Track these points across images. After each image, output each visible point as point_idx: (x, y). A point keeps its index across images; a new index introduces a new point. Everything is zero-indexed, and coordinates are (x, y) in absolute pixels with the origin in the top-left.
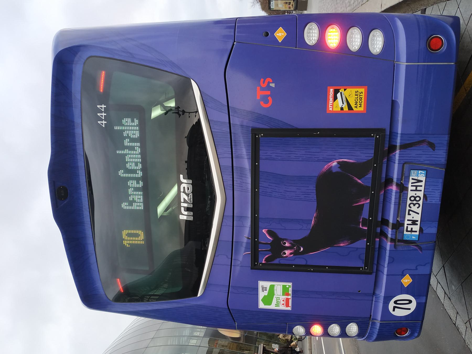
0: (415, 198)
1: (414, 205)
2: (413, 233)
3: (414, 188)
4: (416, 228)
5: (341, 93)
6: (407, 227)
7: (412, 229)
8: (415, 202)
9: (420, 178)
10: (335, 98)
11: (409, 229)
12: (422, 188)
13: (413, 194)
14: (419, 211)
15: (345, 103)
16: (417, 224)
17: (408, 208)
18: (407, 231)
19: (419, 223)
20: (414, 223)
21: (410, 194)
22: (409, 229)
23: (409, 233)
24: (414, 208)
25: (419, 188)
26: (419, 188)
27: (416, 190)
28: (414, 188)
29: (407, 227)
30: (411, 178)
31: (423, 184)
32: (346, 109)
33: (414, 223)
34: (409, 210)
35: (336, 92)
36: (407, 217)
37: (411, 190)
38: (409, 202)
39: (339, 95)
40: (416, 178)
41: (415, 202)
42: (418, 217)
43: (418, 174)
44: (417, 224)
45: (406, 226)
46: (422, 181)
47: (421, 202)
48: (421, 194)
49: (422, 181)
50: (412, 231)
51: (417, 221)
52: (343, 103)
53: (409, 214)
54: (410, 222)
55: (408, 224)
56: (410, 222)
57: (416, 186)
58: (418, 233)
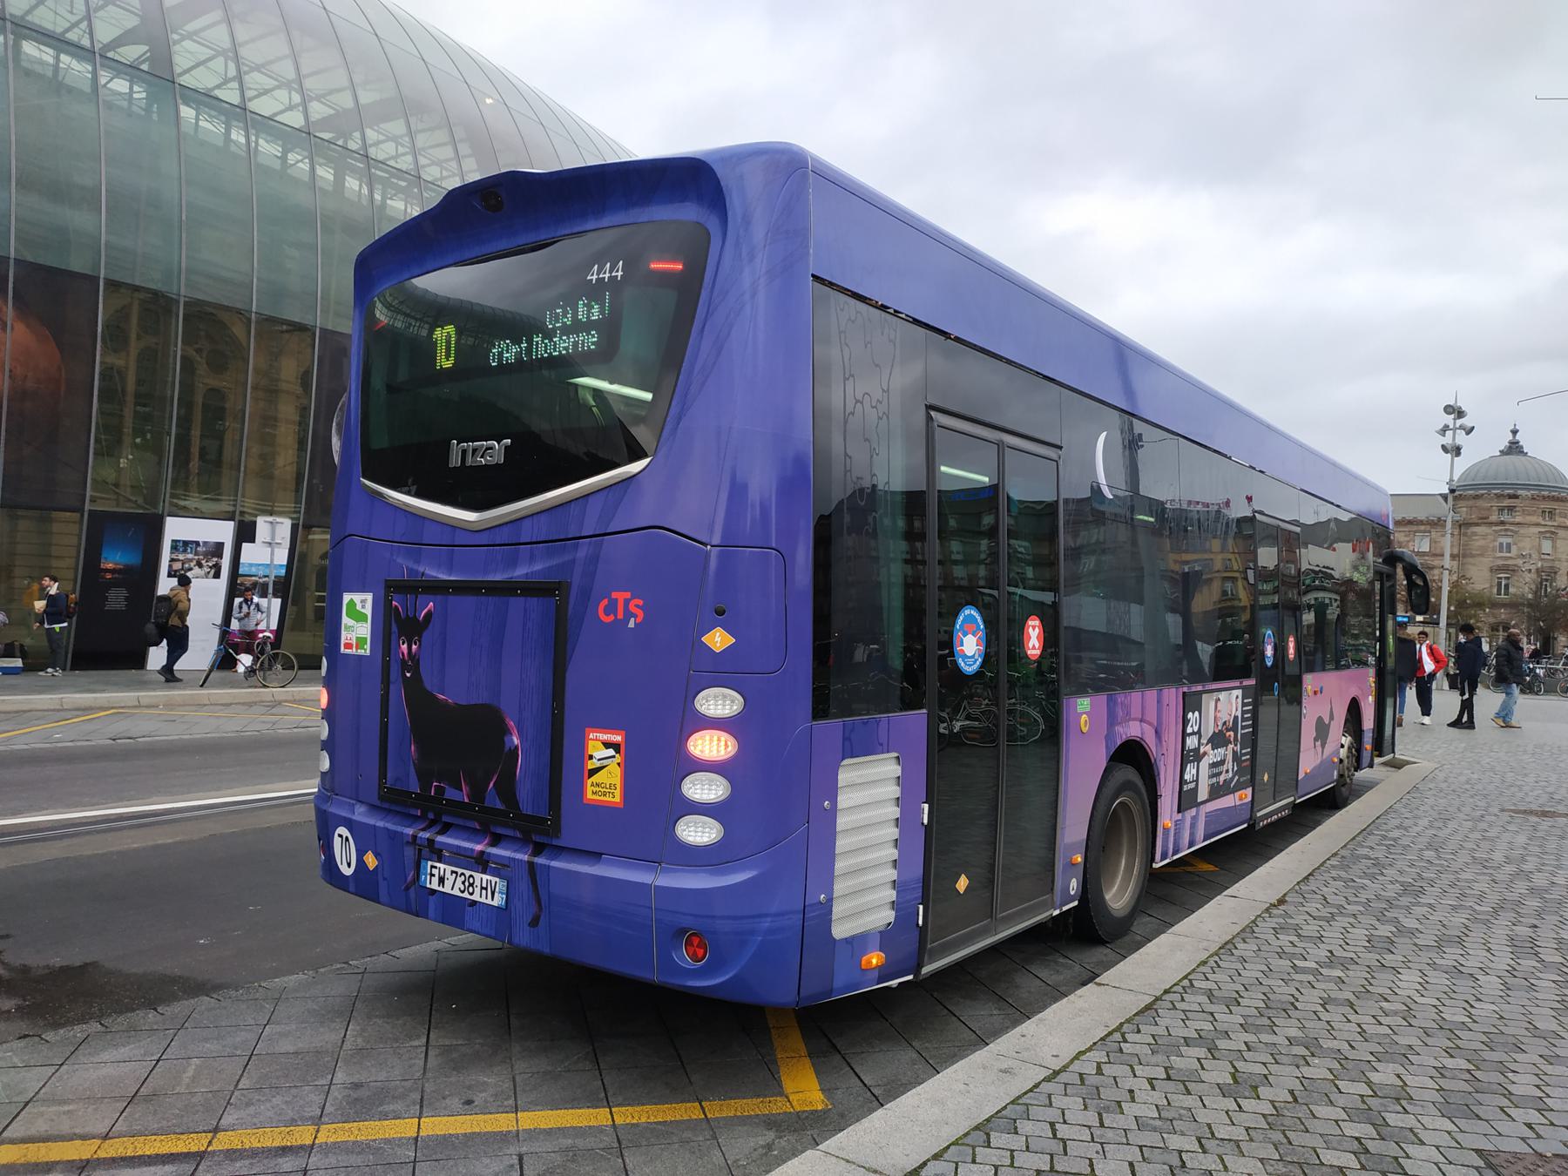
0: (471, 885)
1: (463, 883)
2: (428, 877)
3: (484, 885)
4: (435, 885)
5: (614, 757)
6: (436, 867)
7: (434, 875)
8: (467, 884)
9: (496, 894)
10: (607, 745)
12: (483, 900)
13: (477, 883)
14: (456, 892)
15: (598, 764)
17: (460, 871)
18: (432, 867)
19: (440, 889)
20: (442, 880)
21: (477, 876)
22: (435, 871)
23: (429, 871)
24: (459, 884)
25: (484, 892)
27: (482, 888)
29: (436, 867)
30: (498, 880)
31: (489, 901)
32: (591, 765)
33: (442, 880)
34: (456, 873)
35: (615, 746)
36: (449, 868)
38: (468, 873)
39: (611, 752)
40: (497, 889)
41: (467, 884)
42: (447, 889)
43: (502, 893)
45: (438, 865)
47: (466, 895)
48: (476, 897)
49: (493, 900)
51: (443, 887)
52: (599, 760)
53: (453, 872)
54: (442, 873)
56: (442, 873)
57: (486, 889)
58: (428, 886)
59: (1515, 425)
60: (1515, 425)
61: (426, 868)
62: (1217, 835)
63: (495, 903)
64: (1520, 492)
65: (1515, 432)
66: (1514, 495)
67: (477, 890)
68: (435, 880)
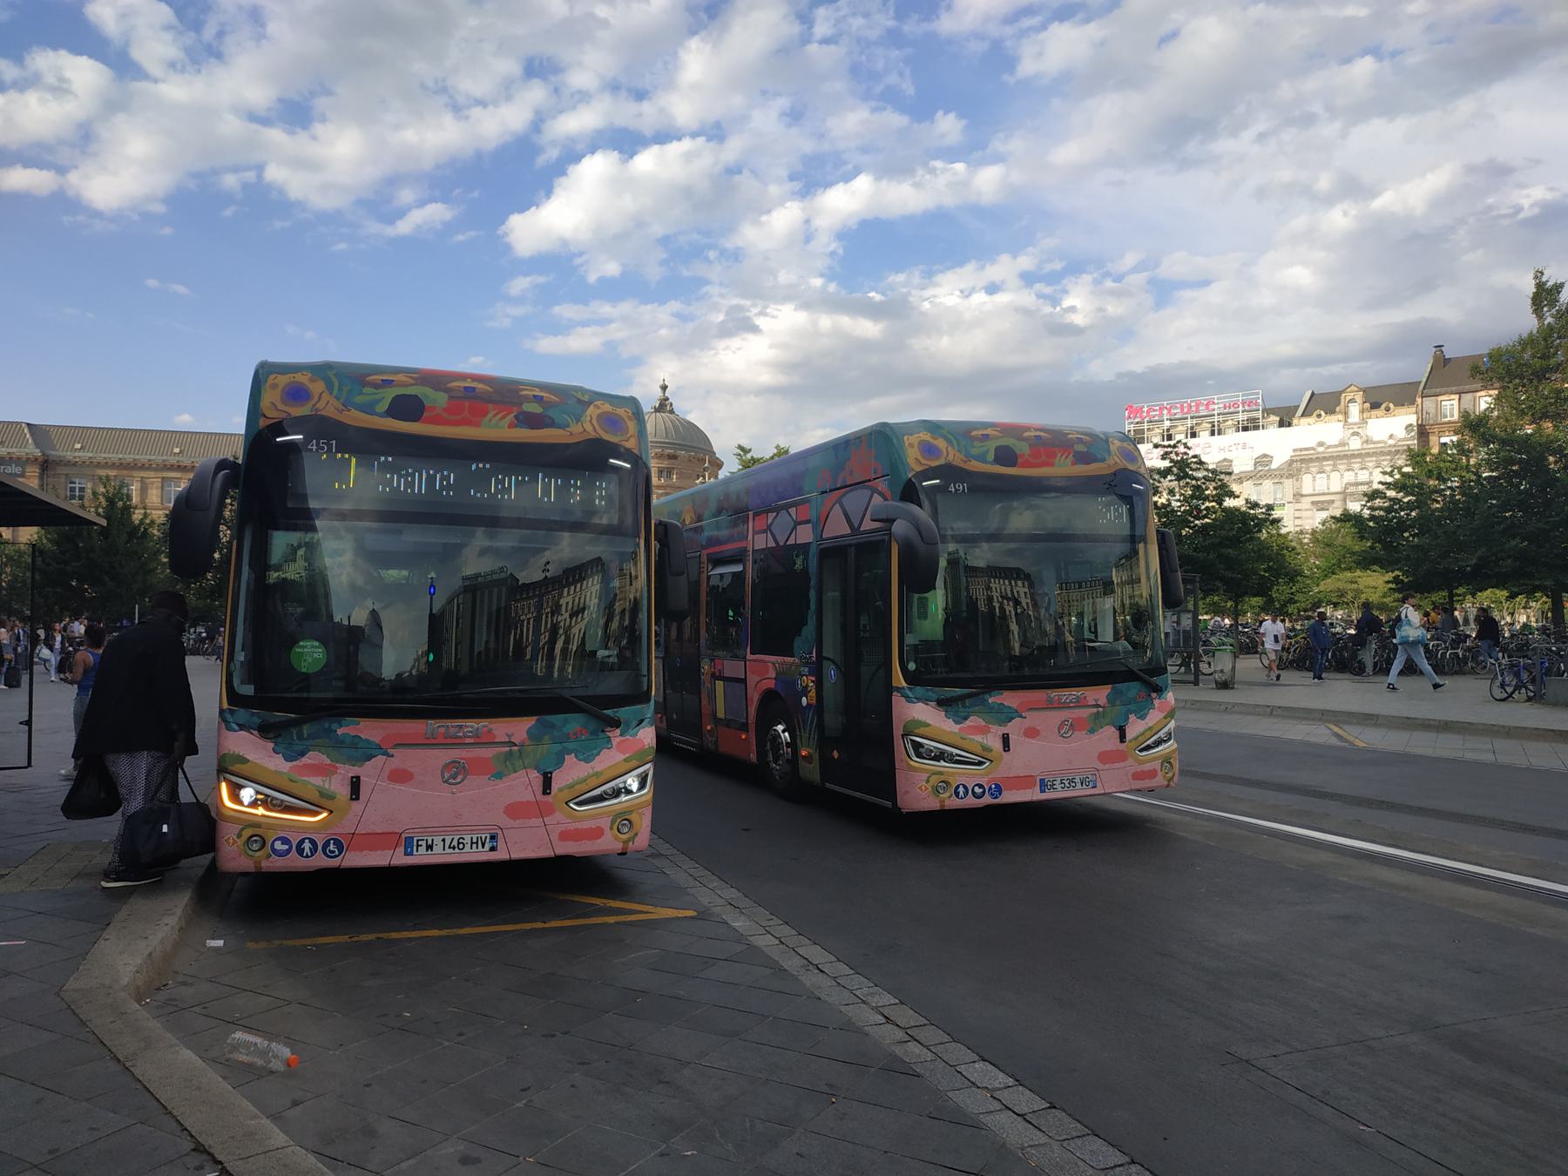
2: (415, 848)
3: (475, 840)
11: (420, 843)
16: (427, 850)
18: (418, 841)
20: (429, 847)
22: (420, 843)
23: (415, 843)
25: (474, 846)
26: (474, 846)
27: (472, 843)
28: (475, 840)
33: (429, 847)
37: (472, 838)
44: (427, 850)
46: (483, 847)
49: (483, 847)
51: (432, 850)
54: (430, 842)
55: (427, 840)
56: (430, 842)
57: (477, 843)
59: (664, 380)
60: (664, 380)
64: (679, 452)
65: (664, 388)
66: (674, 456)
68: (422, 850)
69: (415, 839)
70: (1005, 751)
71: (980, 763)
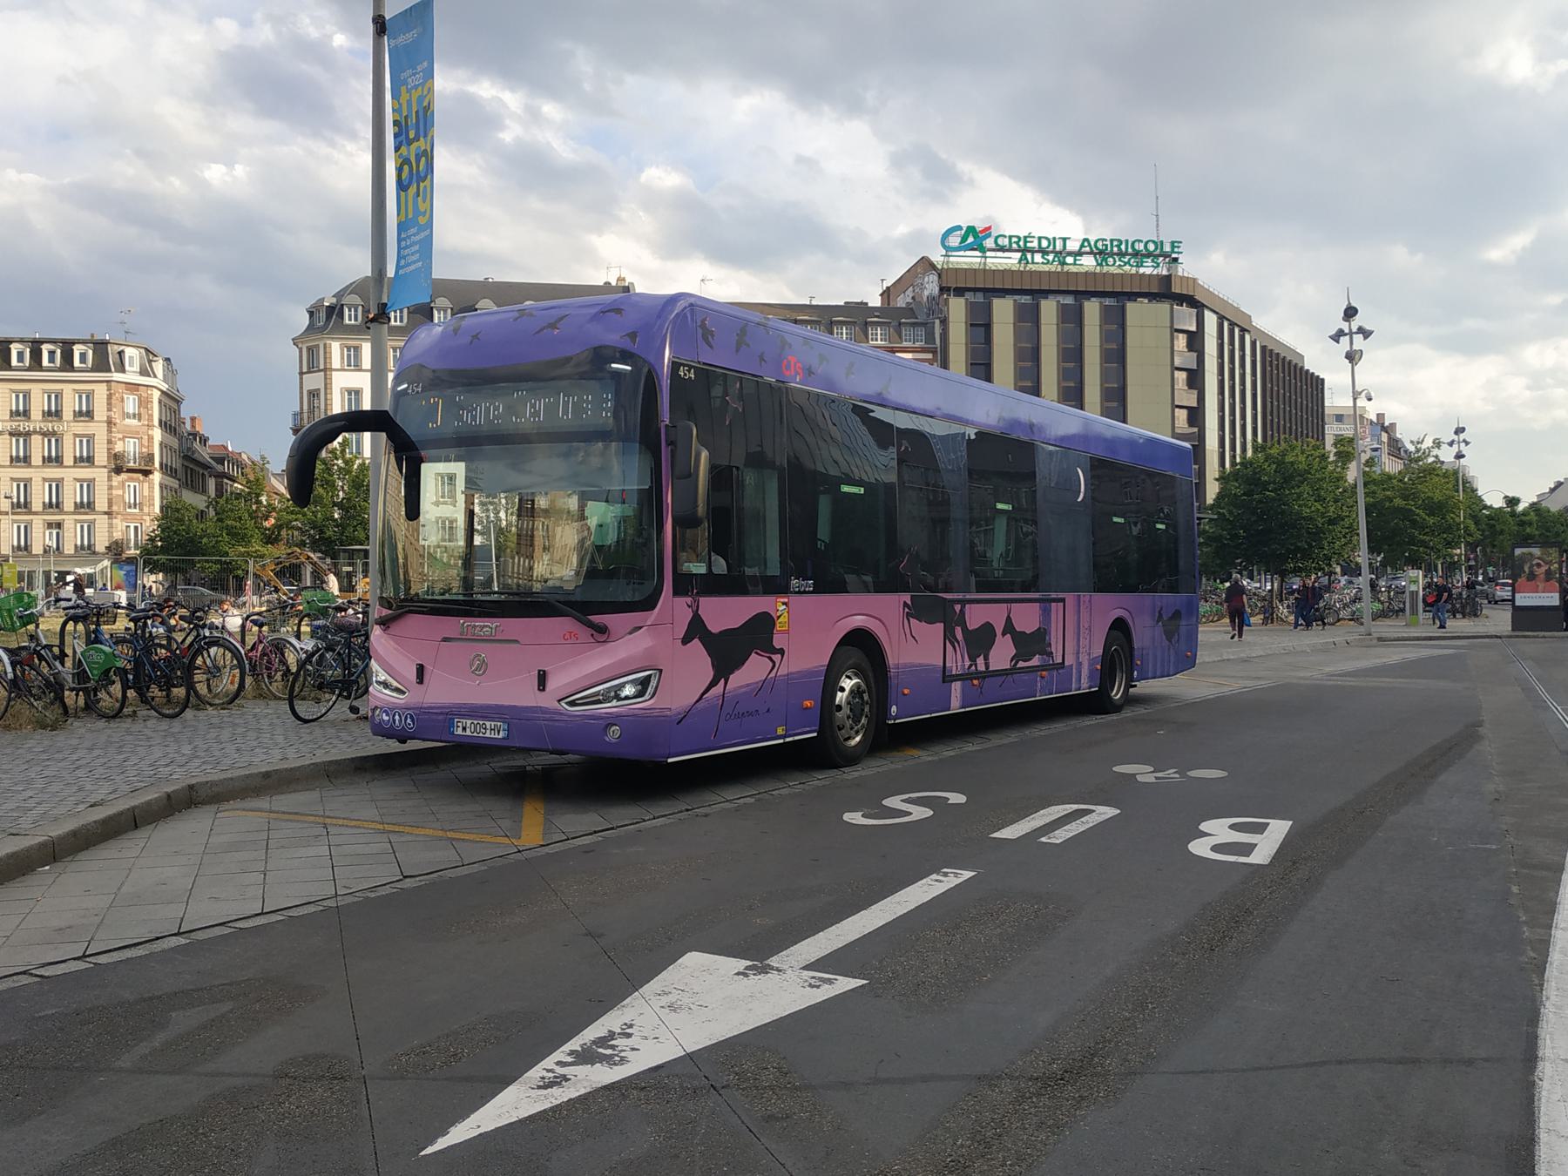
4: (460, 732)
9: (501, 732)
11: (460, 724)
13: (488, 727)
19: (464, 734)
20: (464, 729)
21: (488, 724)
22: (460, 724)
25: (493, 732)
26: (493, 732)
27: (491, 730)
31: (496, 736)
33: (464, 729)
36: (469, 722)
42: (468, 733)
47: (481, 735)
48: (488, 735)
50: (458, 727)
58: (456, 733)
61: (453, 723)
62: (763, 741)
63: (500, 736)
67: (488, 731)
68: (460, 729)
69: (456, 720)
70: (539, 689)
71: (404, 693)
